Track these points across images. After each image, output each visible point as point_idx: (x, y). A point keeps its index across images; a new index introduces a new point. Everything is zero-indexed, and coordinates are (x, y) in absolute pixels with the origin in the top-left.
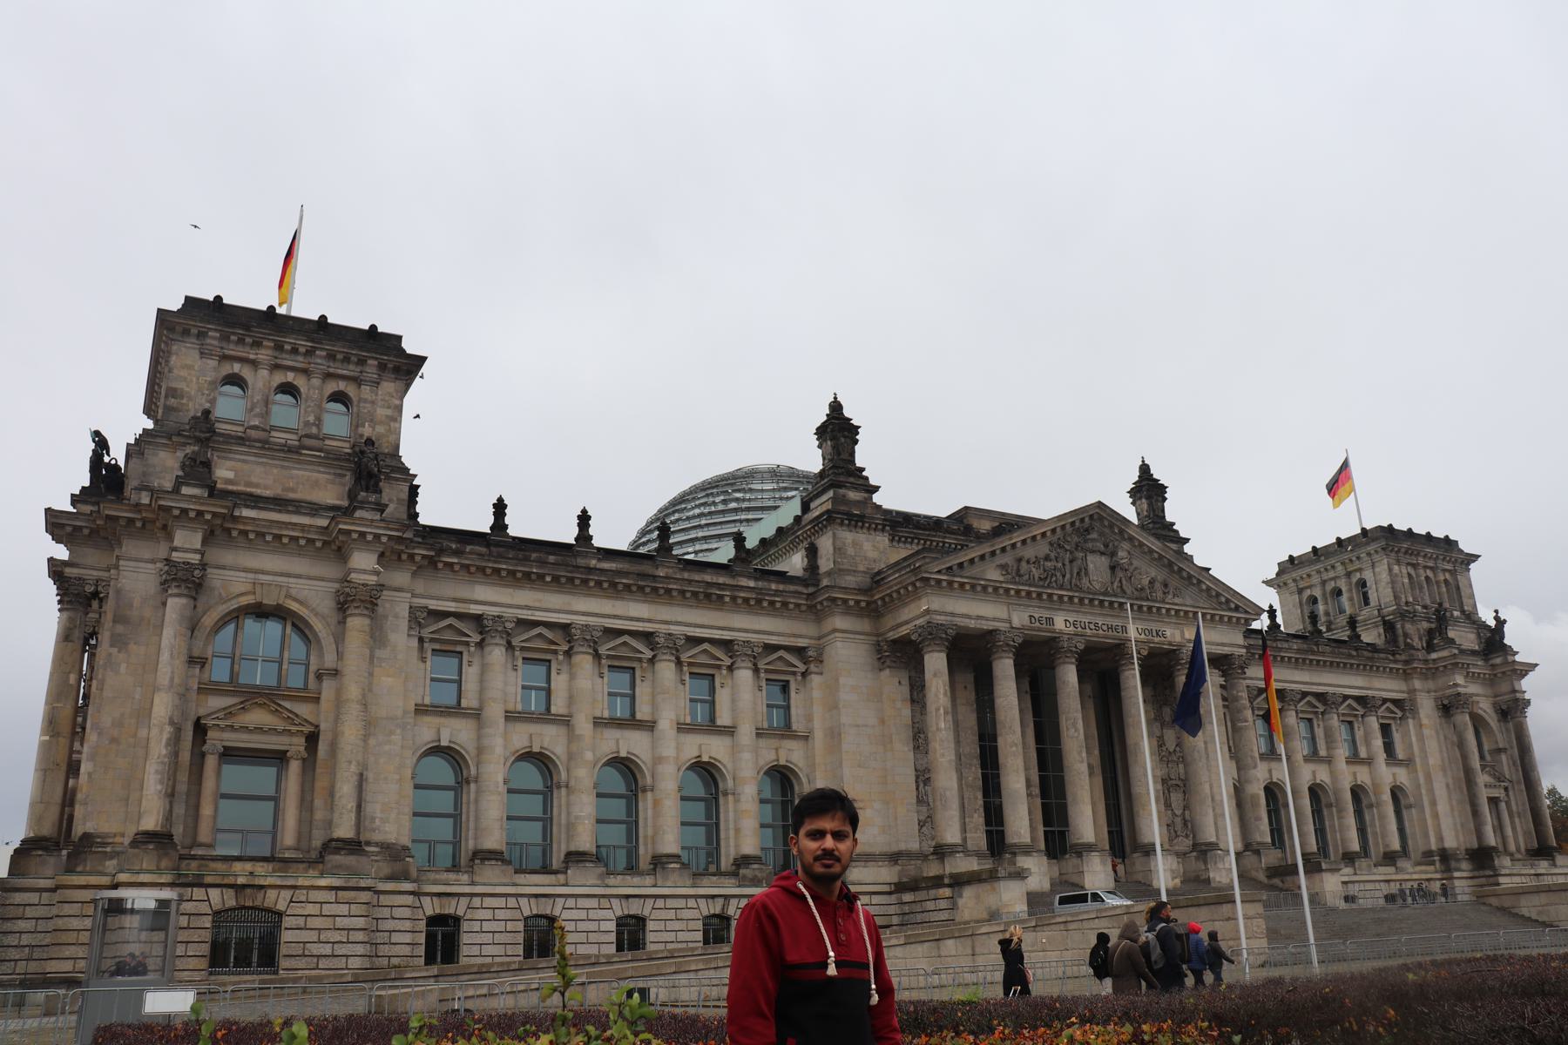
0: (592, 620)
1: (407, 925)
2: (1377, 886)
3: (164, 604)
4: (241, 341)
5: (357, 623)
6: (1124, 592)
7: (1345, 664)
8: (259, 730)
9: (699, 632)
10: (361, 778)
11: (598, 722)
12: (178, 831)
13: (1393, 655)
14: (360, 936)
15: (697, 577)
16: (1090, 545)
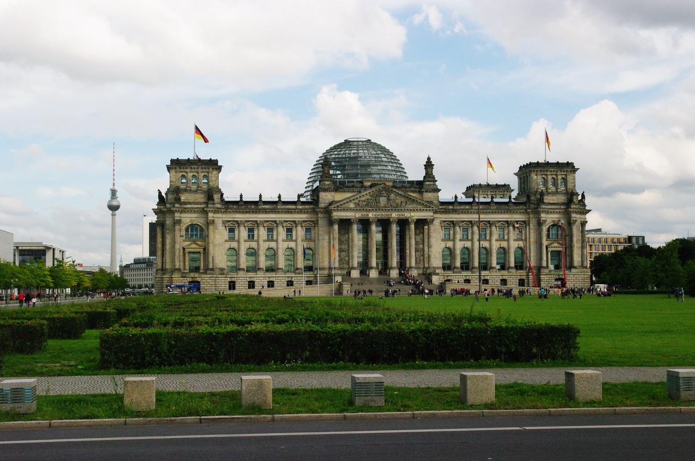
0: (262, 219)
1: (224, 283)
2: (498, 277)
3: (174, 226)
4: (183, 168)
5: (211, 227)
6: (391, 206)
7: (498, 212)
8: (194, 248)
9: (287, 220)
10: (213, 257)
11: (264, 241)
12: (182, 268)
13: (526, 206)
14: (214, 285)
15: (287, 207)
16: (381, 195)
